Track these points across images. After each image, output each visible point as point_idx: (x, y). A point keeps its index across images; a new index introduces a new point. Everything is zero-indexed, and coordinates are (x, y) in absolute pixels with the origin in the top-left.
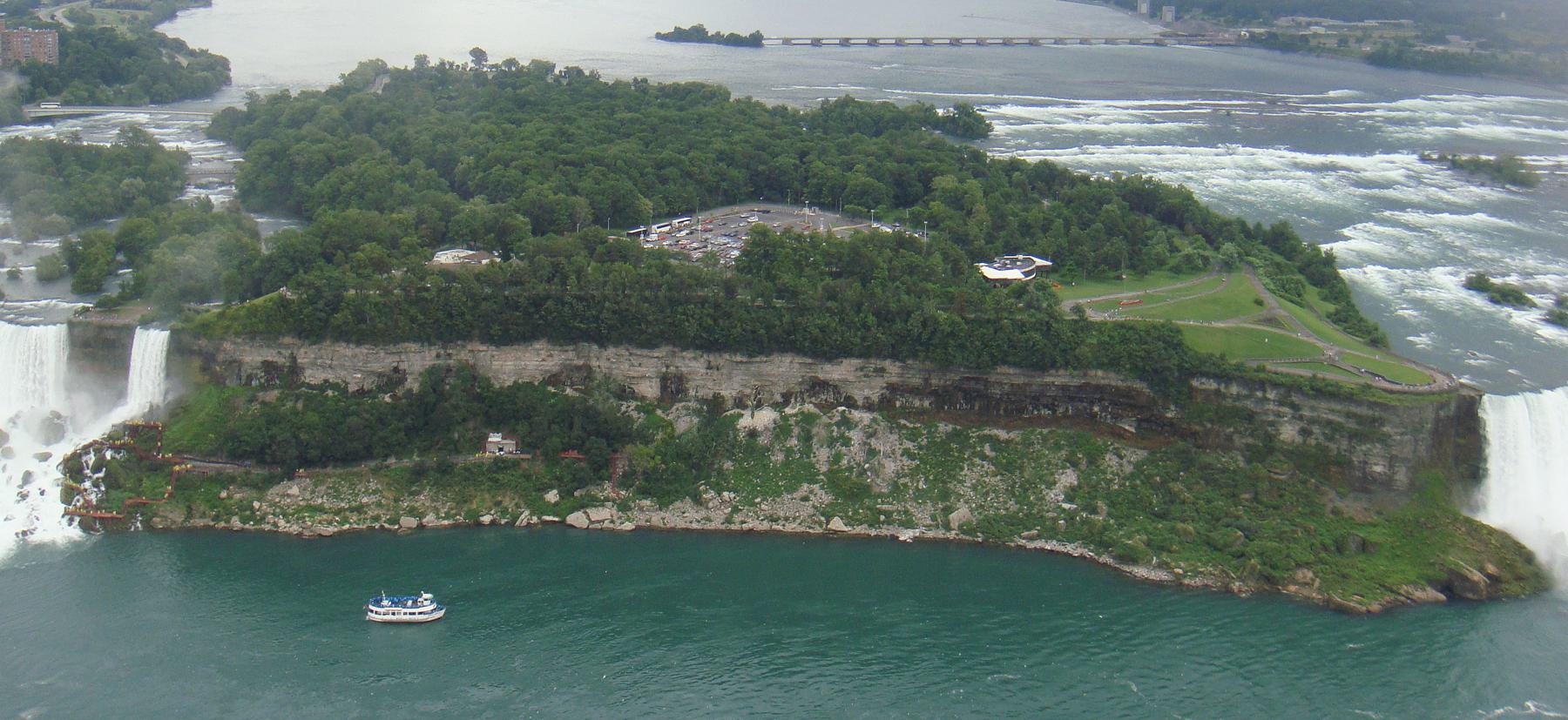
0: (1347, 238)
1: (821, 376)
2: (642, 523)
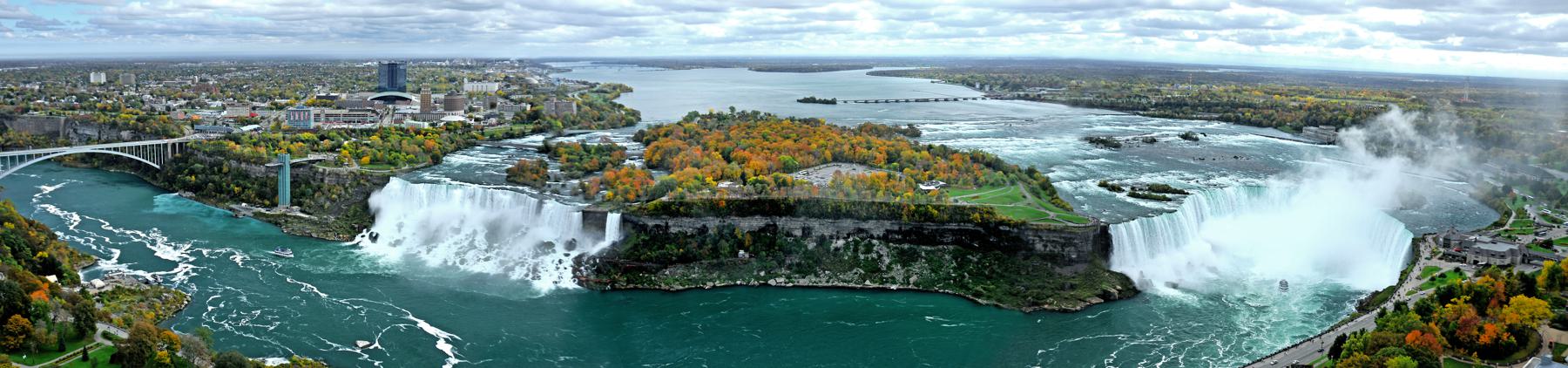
0: (1053, 171)
1: (861, 227)
2: (796, 284)
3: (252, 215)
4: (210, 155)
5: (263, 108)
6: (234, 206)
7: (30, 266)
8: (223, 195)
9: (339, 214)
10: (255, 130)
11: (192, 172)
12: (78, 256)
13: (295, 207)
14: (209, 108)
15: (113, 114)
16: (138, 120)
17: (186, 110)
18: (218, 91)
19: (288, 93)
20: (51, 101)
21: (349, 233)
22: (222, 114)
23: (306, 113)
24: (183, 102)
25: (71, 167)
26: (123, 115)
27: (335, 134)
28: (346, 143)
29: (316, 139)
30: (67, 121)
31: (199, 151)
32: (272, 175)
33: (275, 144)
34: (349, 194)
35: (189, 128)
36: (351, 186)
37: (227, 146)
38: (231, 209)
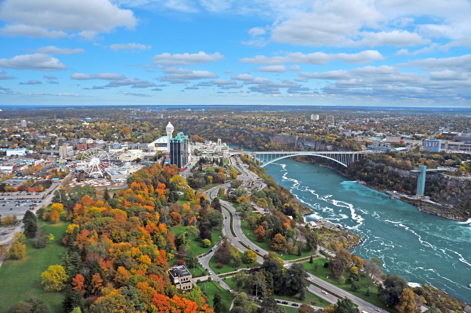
3: (399, 198)
4: (377, 162)
5: (408, 138)
6: (388, 192)
7: (280, 210)
8: (382, 185)
9: (457, 204)
10: (403, 150)
11: (365, 171)
12: (303, 208)
13: (427, 197)
14: (375, 136)
15: (323, 136)
16: (336, 140)
17: (362, 136)
18: (381, 127)
19: (423, 130)
20: (292, 128)
21: (463, 216)
22: (383, 140)
23: (436, 143)
24: (361, 132)
25: (300, 162)
26: (328, 137)
27: (455, 156)
28: (463, 162)
29: (443, 158)
30: (299, 138)
31: (370, 159)
32: (414, 177)
33: (417, 159)
34: (464, 193)
35: (365, 146)
36: (466, 188)
37: (388, 158)
38: (387, 193)
